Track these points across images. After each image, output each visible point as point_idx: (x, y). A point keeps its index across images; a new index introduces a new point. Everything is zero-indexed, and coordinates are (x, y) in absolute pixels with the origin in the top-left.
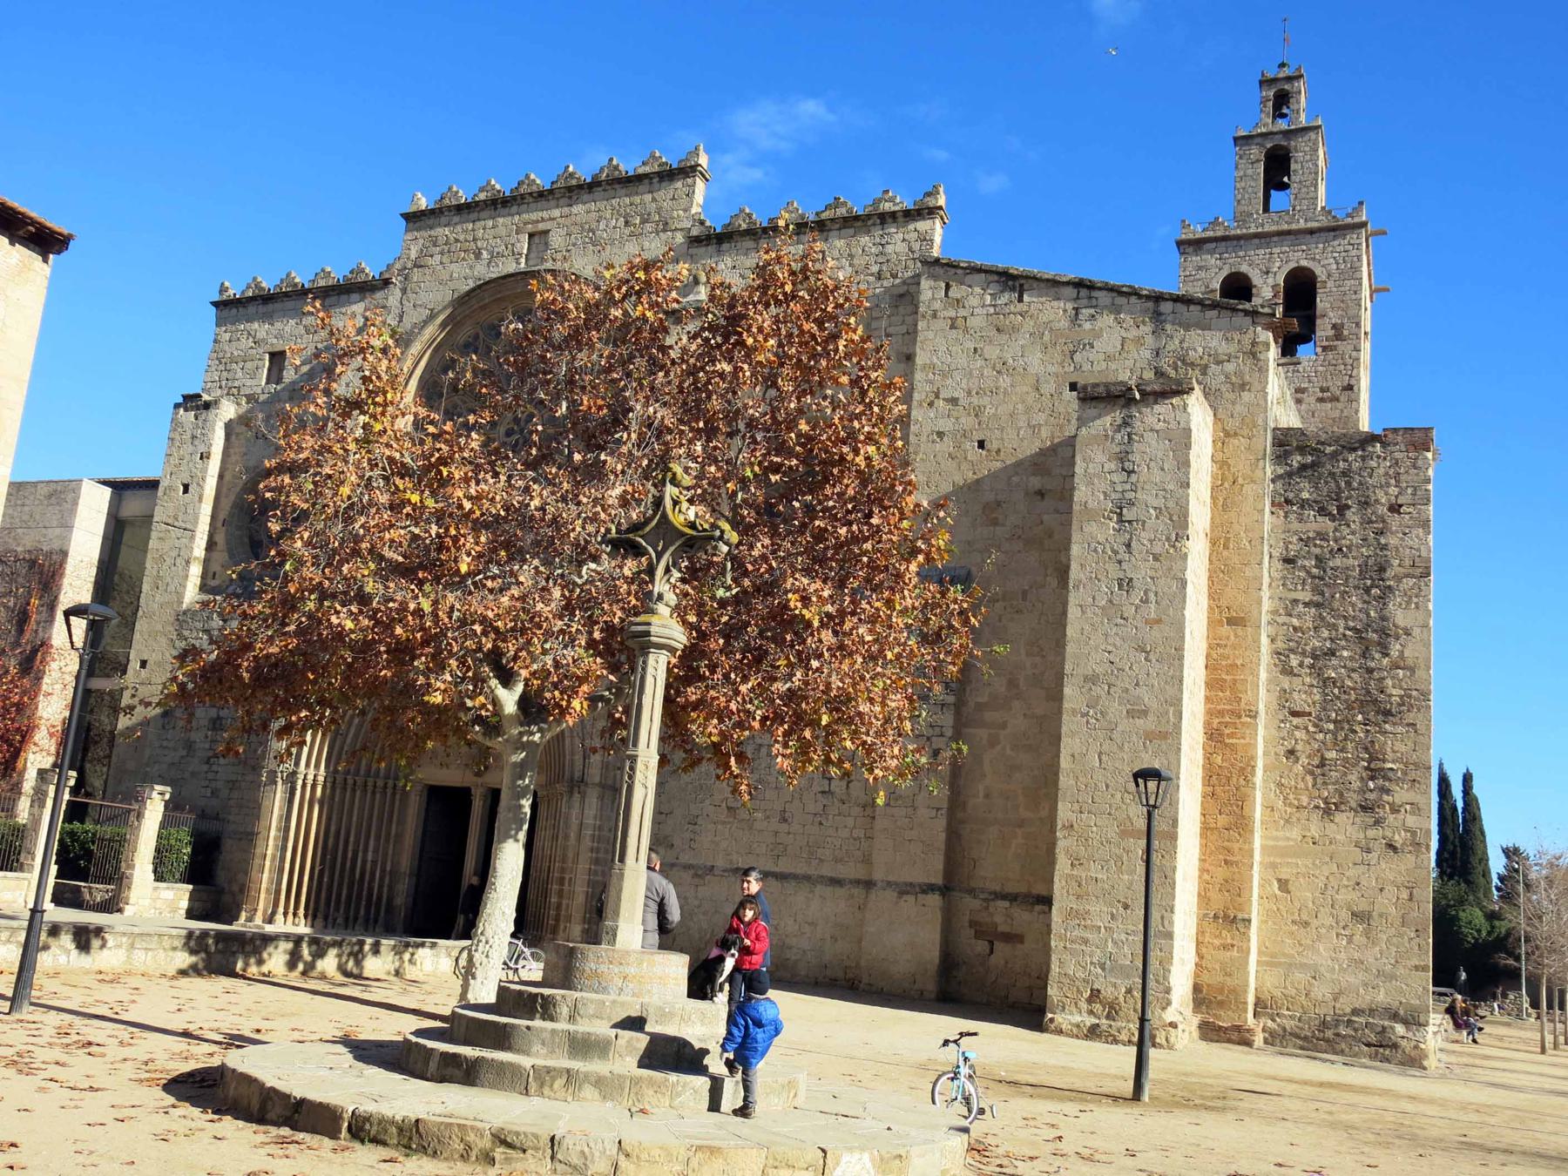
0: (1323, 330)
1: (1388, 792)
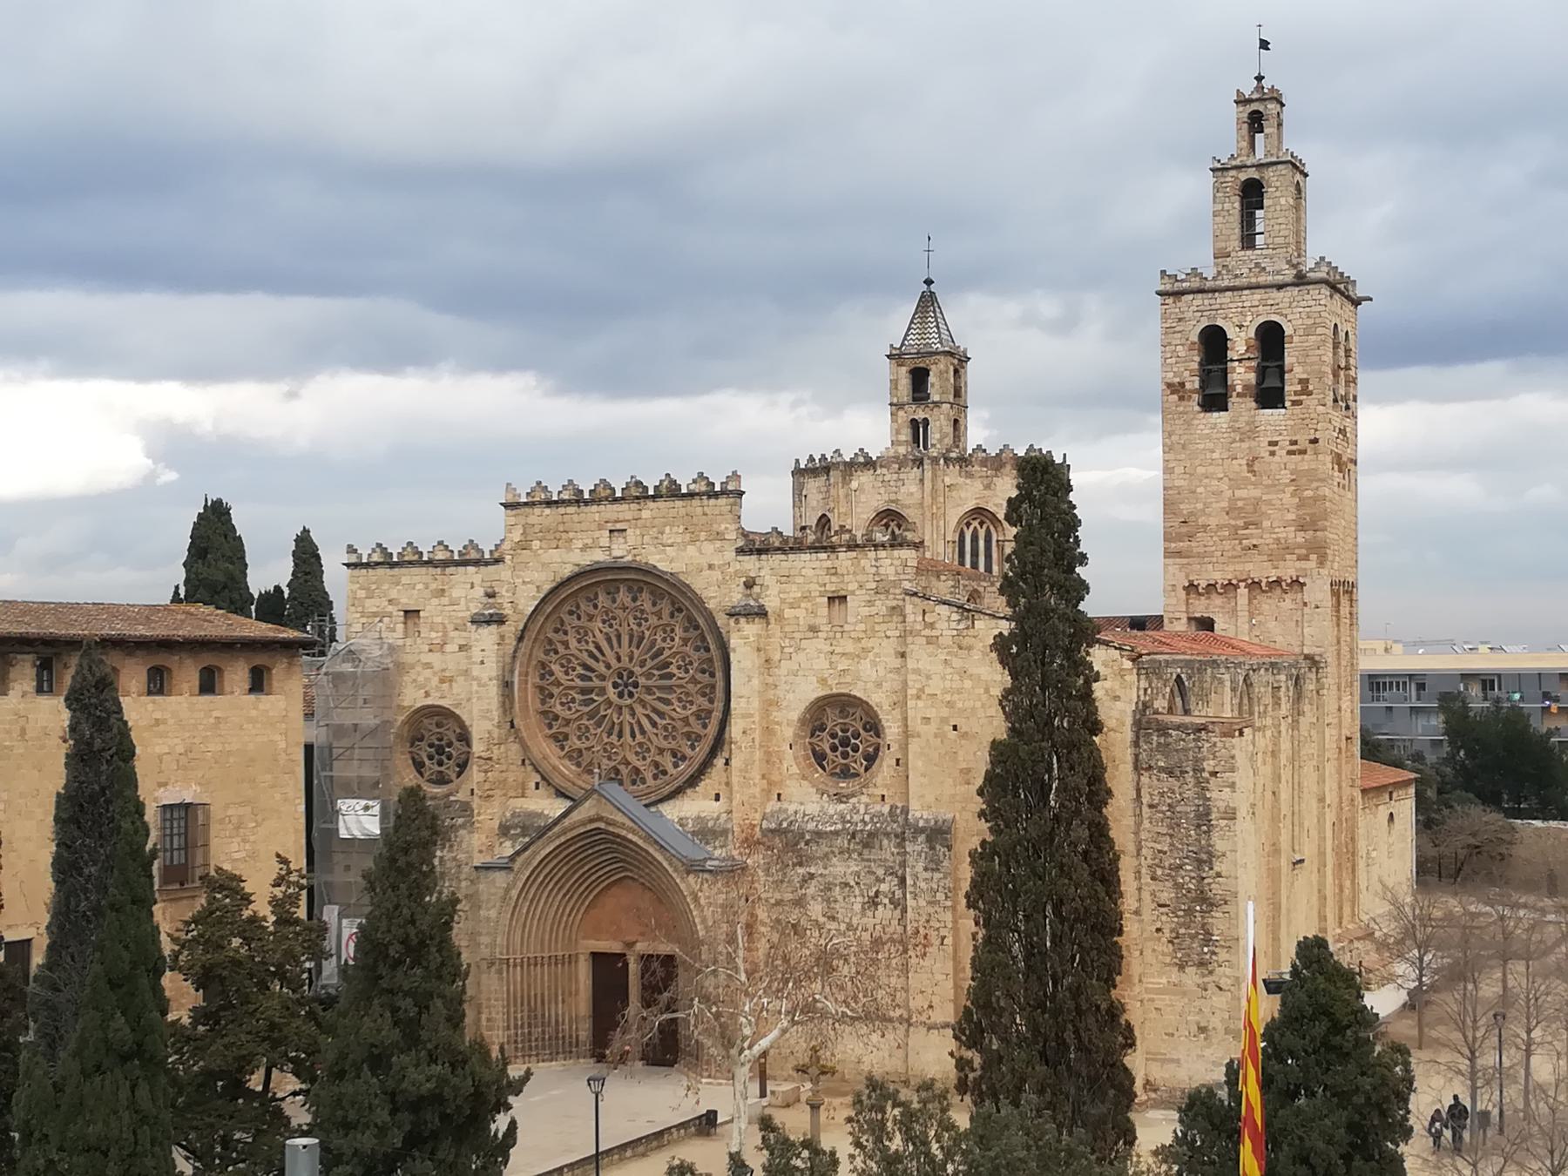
0: (1290, 388)
1: (1214, 953)
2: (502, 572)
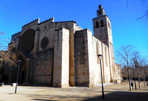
0: (104, 25)
1: (85, 61)
2: (21, 33)
